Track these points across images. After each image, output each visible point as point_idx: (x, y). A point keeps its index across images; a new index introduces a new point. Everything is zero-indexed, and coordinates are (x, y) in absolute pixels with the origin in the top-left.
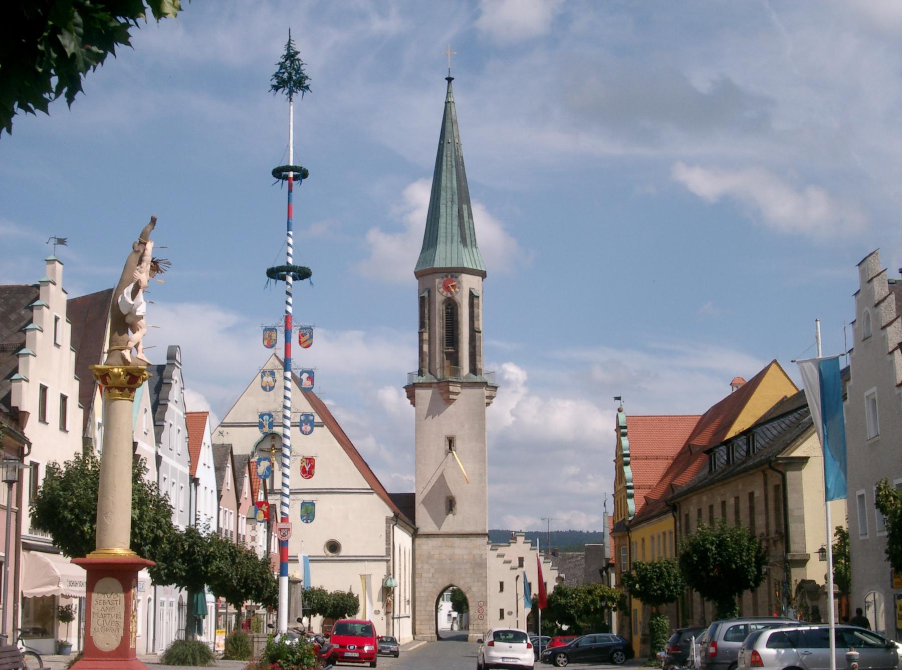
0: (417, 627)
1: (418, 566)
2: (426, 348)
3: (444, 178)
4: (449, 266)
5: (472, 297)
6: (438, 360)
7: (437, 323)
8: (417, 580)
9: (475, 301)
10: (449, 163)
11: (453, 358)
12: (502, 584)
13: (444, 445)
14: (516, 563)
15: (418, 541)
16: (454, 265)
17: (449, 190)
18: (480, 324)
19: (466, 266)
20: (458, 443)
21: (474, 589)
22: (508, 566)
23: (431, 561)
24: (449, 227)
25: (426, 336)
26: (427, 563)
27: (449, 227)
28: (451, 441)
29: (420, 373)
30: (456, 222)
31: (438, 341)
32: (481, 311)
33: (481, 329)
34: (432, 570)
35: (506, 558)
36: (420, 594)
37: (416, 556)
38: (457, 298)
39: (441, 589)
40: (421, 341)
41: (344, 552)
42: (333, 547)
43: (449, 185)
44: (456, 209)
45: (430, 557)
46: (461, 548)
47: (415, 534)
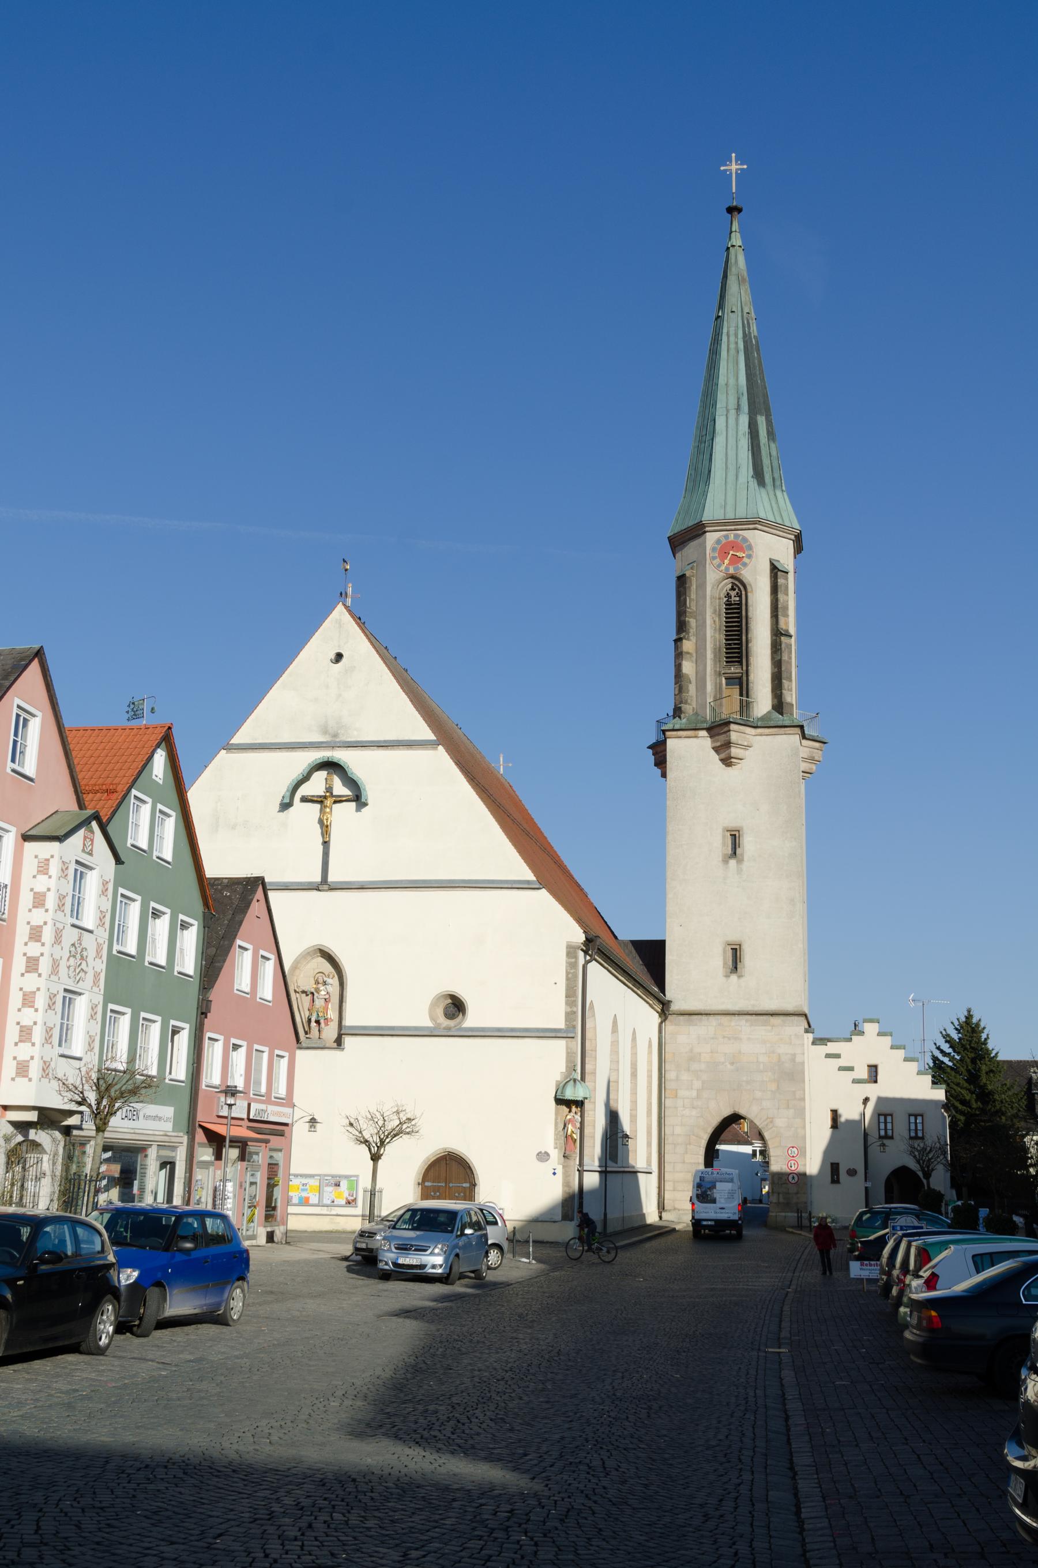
0: (668, 1196)
1: (670, 1075)
2: (688, 667)
3: (723, 370)
4: (730, 515)
5: (775, 570)
6: (710, 687)
7: (709, 622)
8: (668, 1103)
9: (781, 581)
10: (732, 346)
11: (742, 683)
13: (719, 844)
14: (864, 1074)
15: (669, 1027)
16: (741, 513)
17: (732, 392)
18: (790, 623)
19: (762, 515)
20: (748, 844)
21: (780, 1122)
22: (850, 1076)
23: (695, 1066)
24: (731, 454)
25: (688, 646)
27: (731, 454)
28: (735, 839)
29: (677, 712)
30: (744, 442)
31: (709, 655)
32: (790, 600)
33: (792, 631)
34: (697, 1084)
35: (842, 1062)
36: (675, 1128)
37: (668, 1056)
38: (746, 574)
40: (679, 655)
41: (472, 1020)
42: (456, 1006)
43: (732, 381)
44: (744, 419)
45: (693, 1057)
46: (756, 1042)
47: (665, 1009)
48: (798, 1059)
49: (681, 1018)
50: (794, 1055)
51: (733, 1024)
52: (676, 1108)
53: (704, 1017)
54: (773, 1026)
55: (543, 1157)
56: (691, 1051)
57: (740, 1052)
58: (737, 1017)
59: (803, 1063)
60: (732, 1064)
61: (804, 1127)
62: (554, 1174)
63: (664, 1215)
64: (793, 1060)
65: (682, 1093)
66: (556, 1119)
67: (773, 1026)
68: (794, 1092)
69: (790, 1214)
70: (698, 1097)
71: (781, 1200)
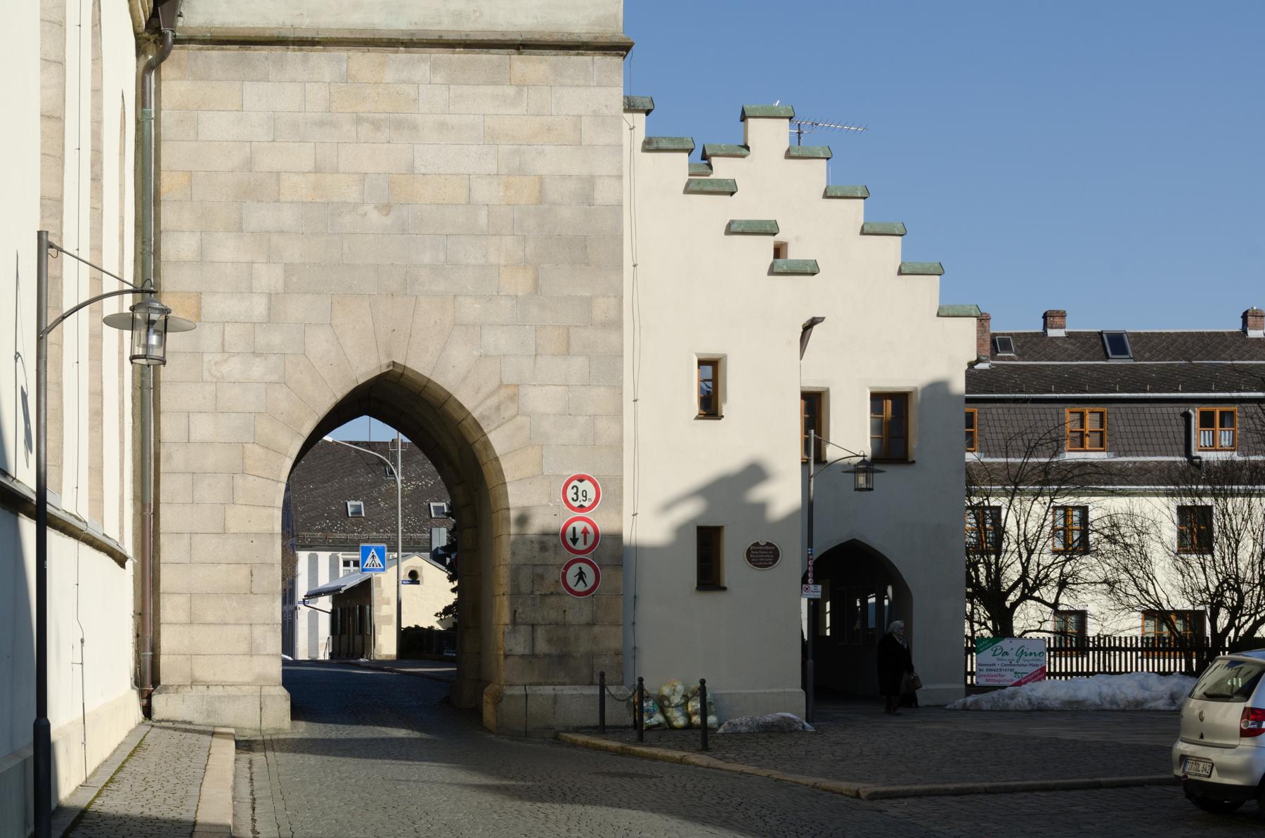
0: (169, 640)
12: (712, 367)
15: (176, 83)
21: (541, 399)
23: (261, 216)
26: (239, 228)
34: (269, 277)
37: (170, 184)
39: (325, 405)
45: (254, 187)
46: (463, 131)
48: (603, 194)
49: (215, 54)
50: (590, 181)
51: (389, 76)
52: (197, 354)
53: (293, 54)
54: (520, 85)
56: (249, 164)
57: (412, 170)
58: (402, 55)
59: (617, 209)
60: (386, 208)
61: (618, 414)
63: (158, 702)
64: (586, 196)
65: (216, 306)
67: (520, 85)
68: (588, 302)
69: (568, 690)
70: (271, 318)
71: (542, 647)
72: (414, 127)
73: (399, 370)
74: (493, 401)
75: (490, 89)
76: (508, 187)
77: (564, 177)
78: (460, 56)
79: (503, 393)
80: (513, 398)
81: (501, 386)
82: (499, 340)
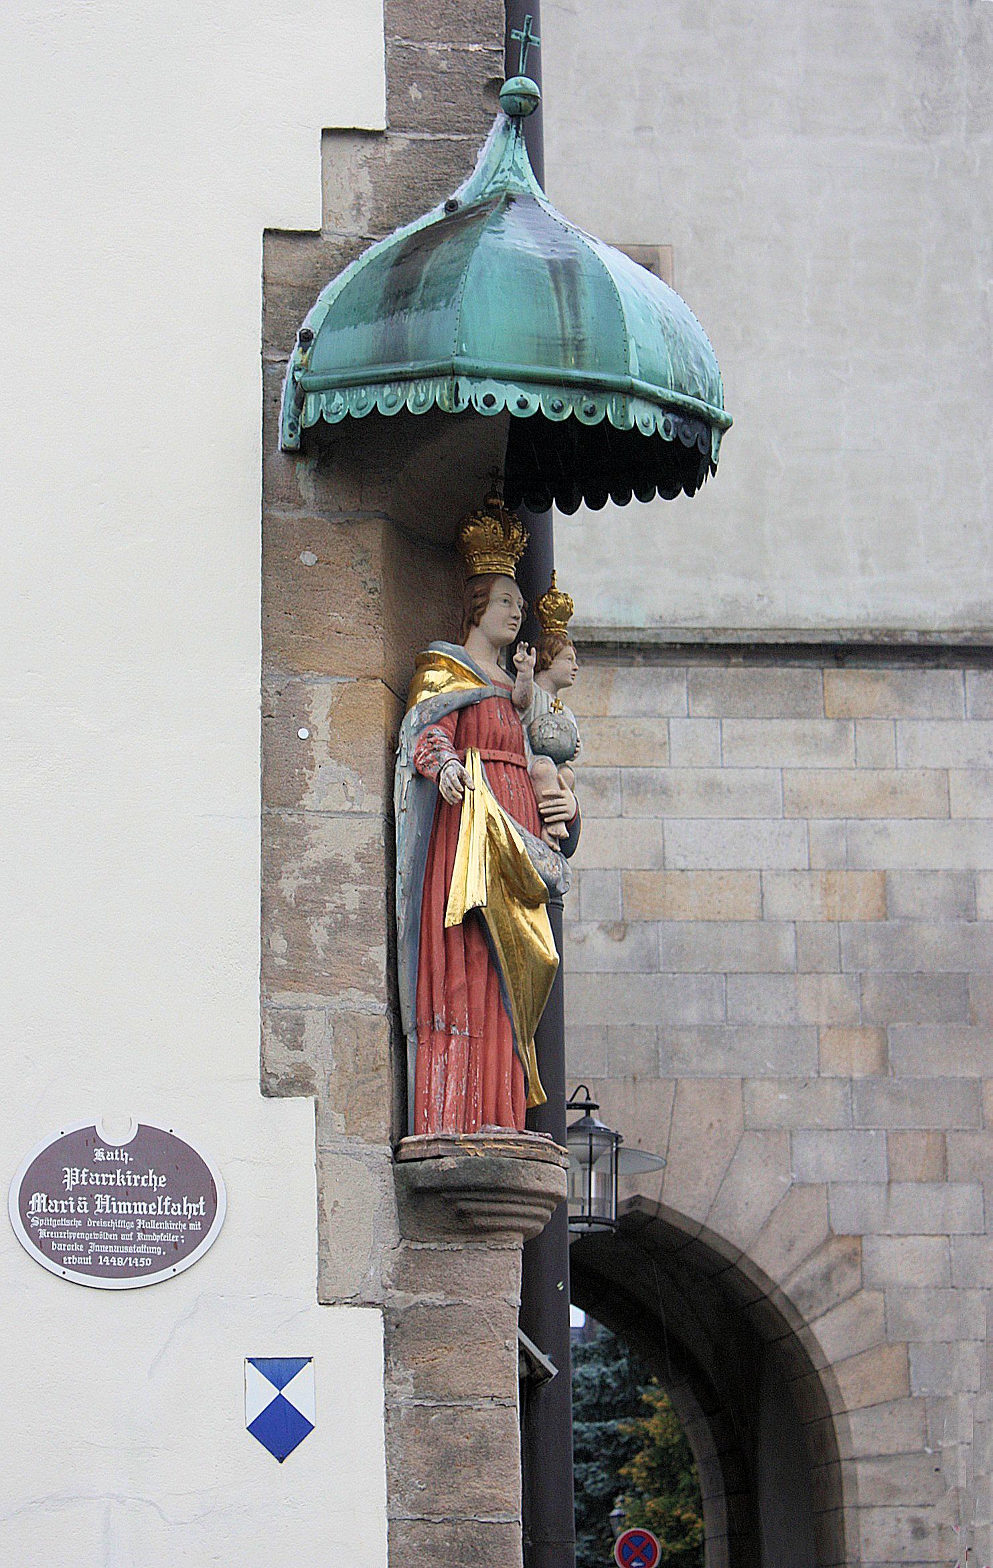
54: (844, 718)
55: (121, 1202)
57: (661, 863)
60: (618, 929)
62: (281, 1430)
66: (279, 715)
67: (844, 718)
72: (665, 791)
73: (650, 1211)
74: (817, 1265)
75: (791, 726)
76: (827, 890)
77: (923, 873)
78: (735, 673)
79: (835, 1249)
80: (853, 1258)
81: (831, 1237)
82: (822, 1156)
